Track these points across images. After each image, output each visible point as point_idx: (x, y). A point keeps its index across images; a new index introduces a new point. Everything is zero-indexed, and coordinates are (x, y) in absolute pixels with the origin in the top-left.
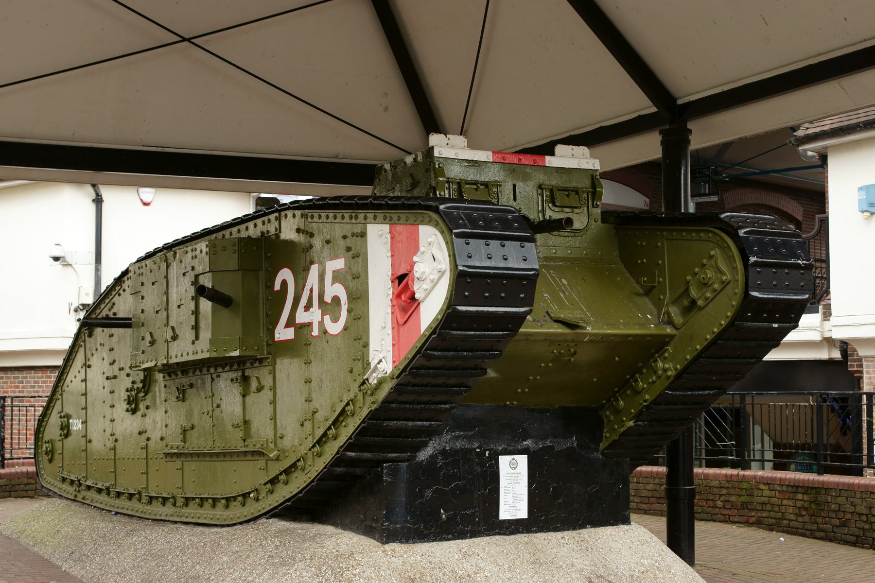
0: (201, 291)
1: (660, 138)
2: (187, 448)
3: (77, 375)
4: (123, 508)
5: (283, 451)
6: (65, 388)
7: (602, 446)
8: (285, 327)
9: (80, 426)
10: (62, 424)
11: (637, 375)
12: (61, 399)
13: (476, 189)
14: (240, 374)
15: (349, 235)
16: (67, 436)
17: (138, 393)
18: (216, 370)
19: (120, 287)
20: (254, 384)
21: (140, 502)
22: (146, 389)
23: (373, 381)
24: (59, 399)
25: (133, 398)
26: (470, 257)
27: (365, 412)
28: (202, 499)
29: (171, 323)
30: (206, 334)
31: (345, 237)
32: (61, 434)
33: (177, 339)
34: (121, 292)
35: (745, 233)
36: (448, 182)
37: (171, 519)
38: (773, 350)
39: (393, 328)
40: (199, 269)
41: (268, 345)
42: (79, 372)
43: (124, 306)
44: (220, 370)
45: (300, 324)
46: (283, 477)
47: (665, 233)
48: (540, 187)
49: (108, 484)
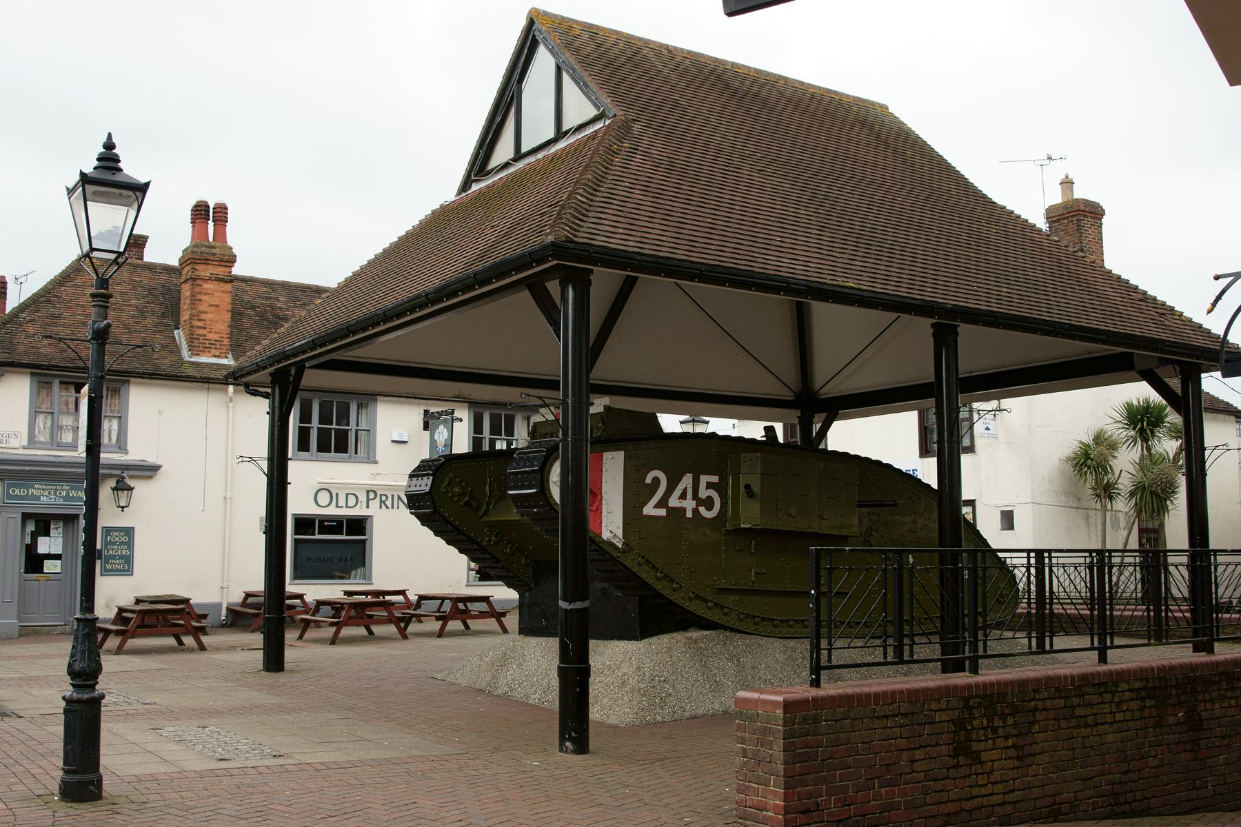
8: (654, 507)
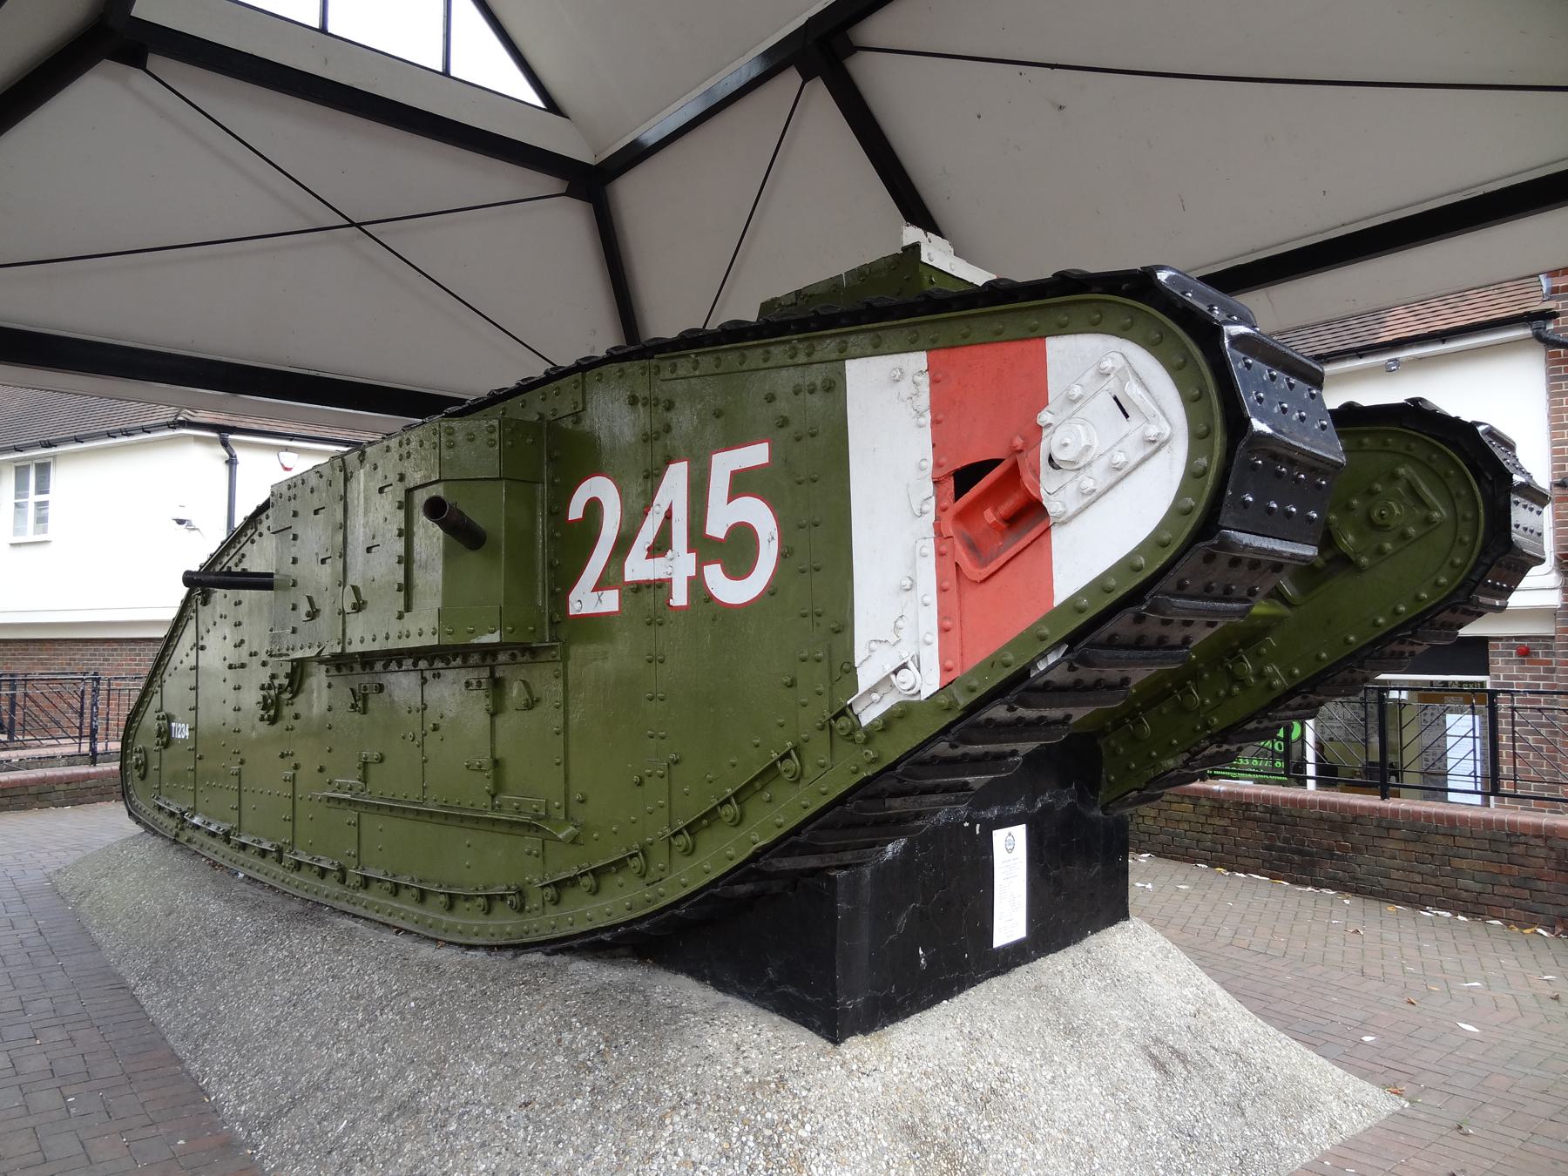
2: (370, 793)
3: (185, 659)
6: (166, 676)
9: (187, 734)
10: (160, 728)
12: (159, 694)
14: (485, 673)
16: (166, 745)
17: (280, 693)
18: (431, 664)
19: (254, 530)
20: (515, 692)
21: (281, 863)
22: (296, 687)
24: (157, 693)
25: (272, 700)
29: (353, 579)
32: (158, 742)
33: (365, 609)
39: (942, 590)
41: (553, 623)
42: (187, 655)
43: (258, 558)
44: (439, 664)
46: (588, 881)
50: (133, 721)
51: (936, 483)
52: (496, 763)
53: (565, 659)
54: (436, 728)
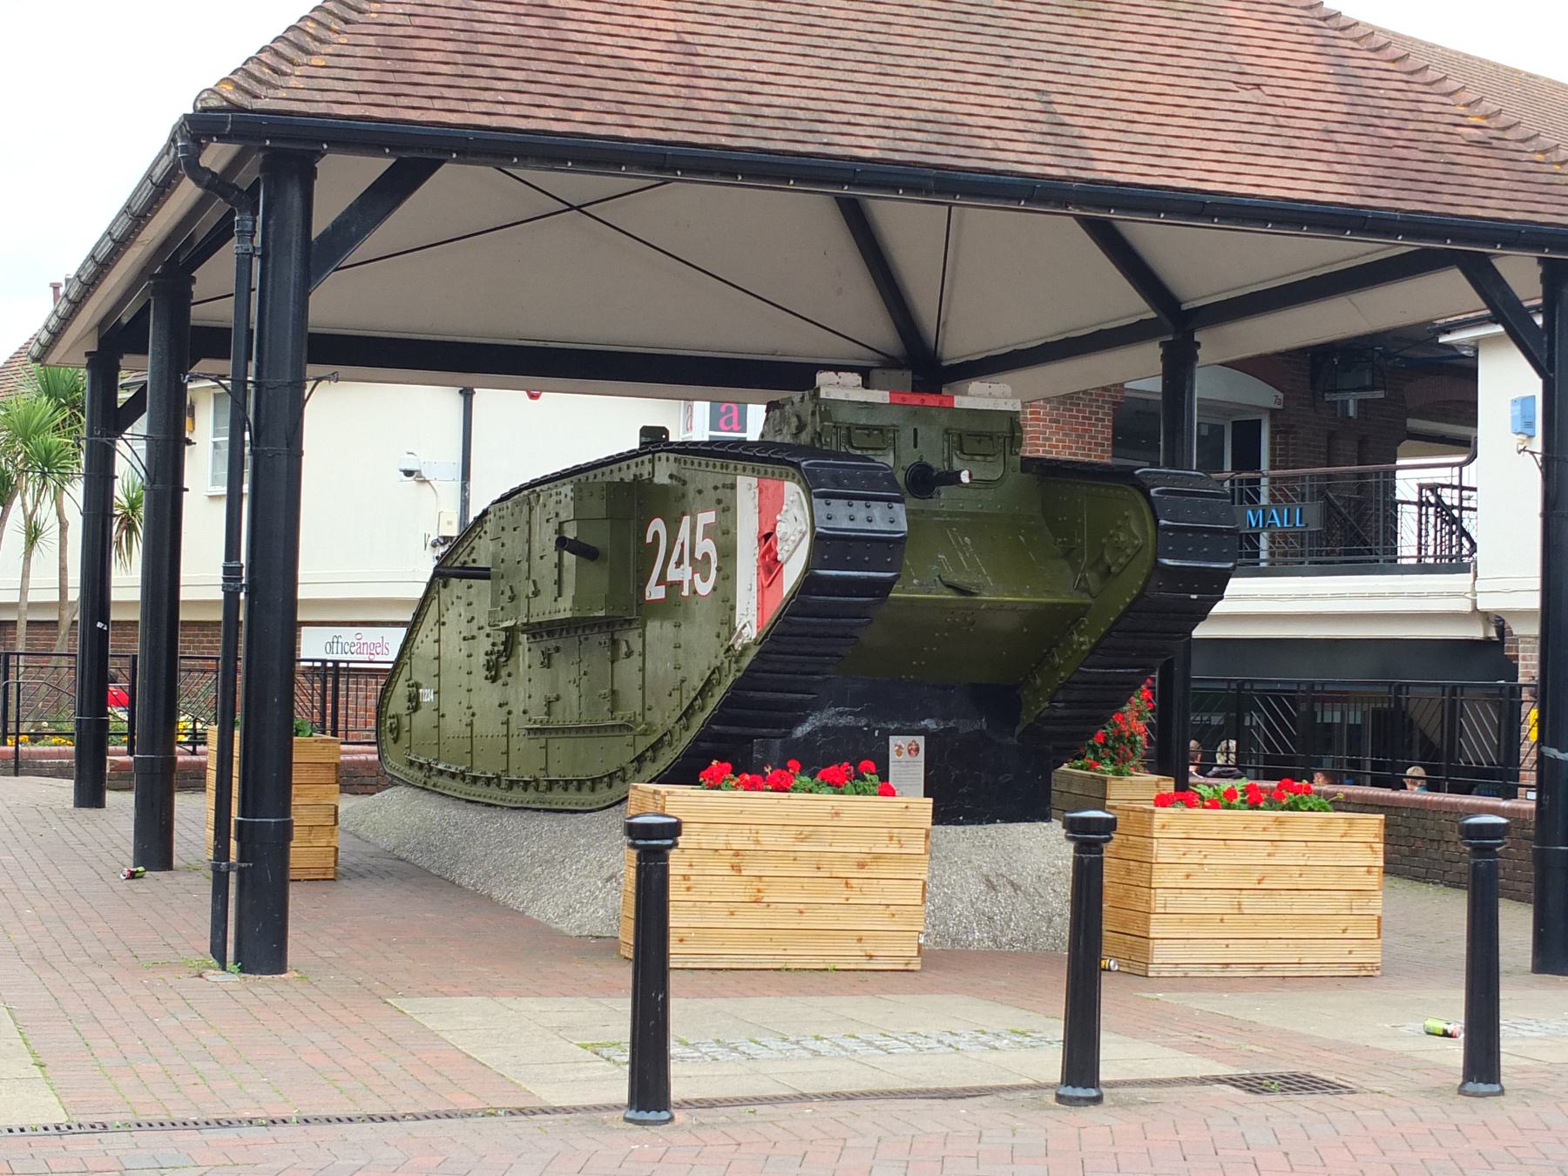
0: (562, 543)
1: (1161, 351)
3: (430, 634)
4: (480, 796)
5: (649, 724)
6: (414, 650)
7: (1018, 730)
8: (657, 585)
10: (410, 695)
11: (1054, 649)
13: (868, 435)
15: (720, 485)
16: (416, 709)
18: (584, 631)
20: (624, 648)
23: (738, 647)
26: (830, 519)
27: (729, 682)
28: (566, 781)
29: (532, 578)
30: (569, 591)
31: (716, 488)
34: (482, 534)
35: (1158, 492)
36: (834, 427)
37: (534, 806)
38: (1201, 624)
39: (758, 590)
40: (563, 517)
41: (639, 605)
43: (483, 553)
45: (671, 582)
47: (1085, 488)
48: (947, 432)
49: (463, 768)
50: (387, 691)
51: (759, 540)
52: (613, 692)
53: (644, 626)
54: (585, 674)
